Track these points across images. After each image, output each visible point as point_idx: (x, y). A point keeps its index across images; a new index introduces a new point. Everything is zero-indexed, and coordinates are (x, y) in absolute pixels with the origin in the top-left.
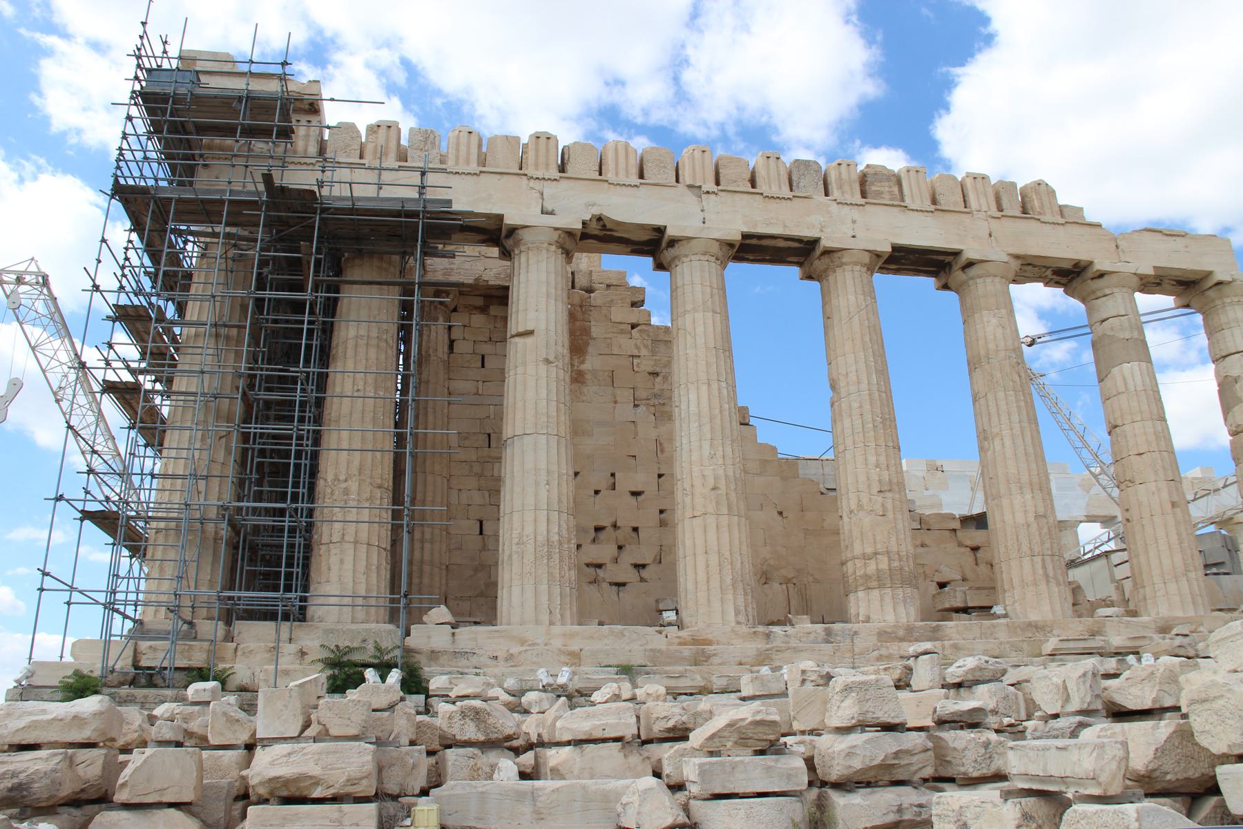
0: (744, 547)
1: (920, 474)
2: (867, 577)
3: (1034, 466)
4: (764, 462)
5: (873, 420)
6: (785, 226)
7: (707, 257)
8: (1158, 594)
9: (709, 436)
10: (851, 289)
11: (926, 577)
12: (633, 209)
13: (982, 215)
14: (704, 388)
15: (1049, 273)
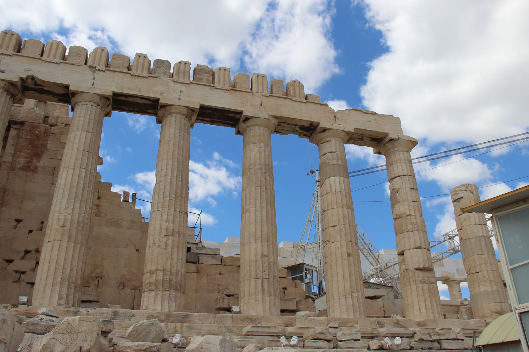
0: (75, 262)
1: (289, 249)
2: (150, 284)
3: (265, 228)
4: (133, 222)
5: (170, 196)
6: (140, 91)
7: (91, 104)
8: (335, 305)
9: (67, 197)
10: (173, 126)
11: (219, 291)
12: (50, 74)
13: (259, 94)
14: (71, 171)
15: (297, 128)
